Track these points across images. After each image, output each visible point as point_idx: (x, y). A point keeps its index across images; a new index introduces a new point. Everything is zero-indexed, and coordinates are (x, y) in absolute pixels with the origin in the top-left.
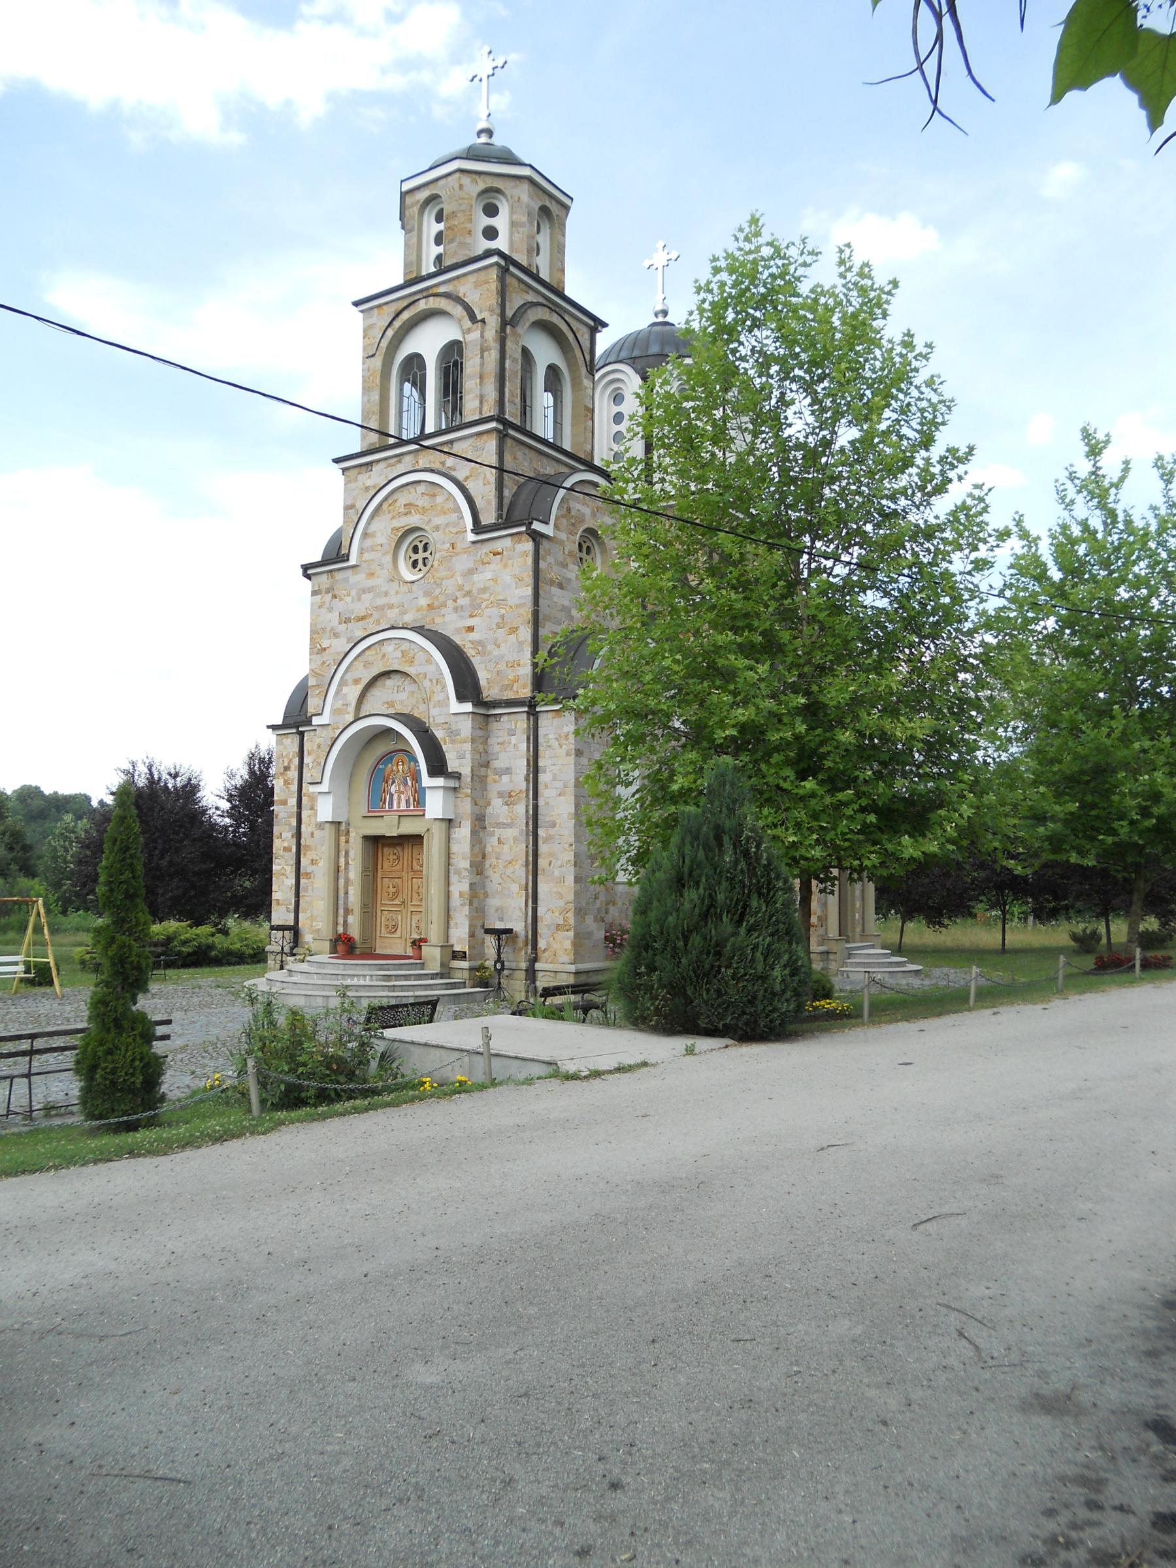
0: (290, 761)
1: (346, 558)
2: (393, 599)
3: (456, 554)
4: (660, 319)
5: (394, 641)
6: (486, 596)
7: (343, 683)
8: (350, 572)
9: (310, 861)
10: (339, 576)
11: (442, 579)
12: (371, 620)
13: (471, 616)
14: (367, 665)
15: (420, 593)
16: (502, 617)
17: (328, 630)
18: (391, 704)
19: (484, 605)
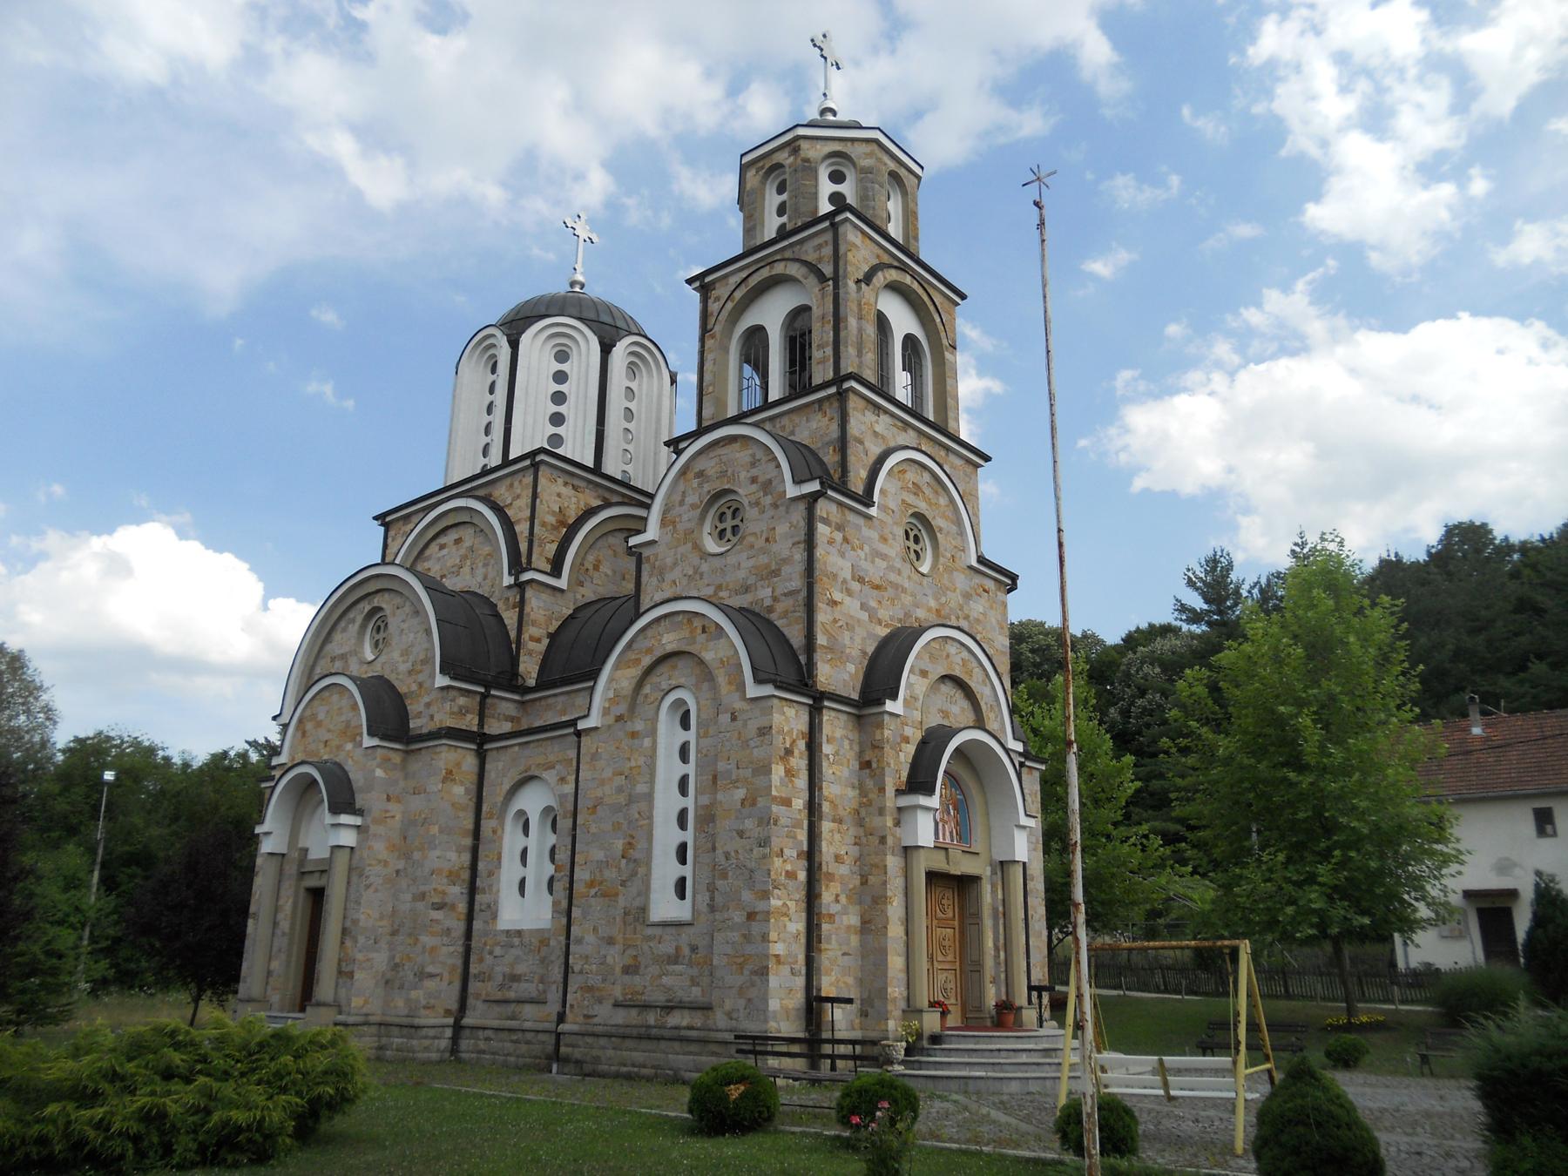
1: (867, 499)
2: (906, 585)
4: (577, 289)
5: (955, 644)
8: (861, 521)
10: (851, 517)
11: (947, 589)
15: (929, 592)
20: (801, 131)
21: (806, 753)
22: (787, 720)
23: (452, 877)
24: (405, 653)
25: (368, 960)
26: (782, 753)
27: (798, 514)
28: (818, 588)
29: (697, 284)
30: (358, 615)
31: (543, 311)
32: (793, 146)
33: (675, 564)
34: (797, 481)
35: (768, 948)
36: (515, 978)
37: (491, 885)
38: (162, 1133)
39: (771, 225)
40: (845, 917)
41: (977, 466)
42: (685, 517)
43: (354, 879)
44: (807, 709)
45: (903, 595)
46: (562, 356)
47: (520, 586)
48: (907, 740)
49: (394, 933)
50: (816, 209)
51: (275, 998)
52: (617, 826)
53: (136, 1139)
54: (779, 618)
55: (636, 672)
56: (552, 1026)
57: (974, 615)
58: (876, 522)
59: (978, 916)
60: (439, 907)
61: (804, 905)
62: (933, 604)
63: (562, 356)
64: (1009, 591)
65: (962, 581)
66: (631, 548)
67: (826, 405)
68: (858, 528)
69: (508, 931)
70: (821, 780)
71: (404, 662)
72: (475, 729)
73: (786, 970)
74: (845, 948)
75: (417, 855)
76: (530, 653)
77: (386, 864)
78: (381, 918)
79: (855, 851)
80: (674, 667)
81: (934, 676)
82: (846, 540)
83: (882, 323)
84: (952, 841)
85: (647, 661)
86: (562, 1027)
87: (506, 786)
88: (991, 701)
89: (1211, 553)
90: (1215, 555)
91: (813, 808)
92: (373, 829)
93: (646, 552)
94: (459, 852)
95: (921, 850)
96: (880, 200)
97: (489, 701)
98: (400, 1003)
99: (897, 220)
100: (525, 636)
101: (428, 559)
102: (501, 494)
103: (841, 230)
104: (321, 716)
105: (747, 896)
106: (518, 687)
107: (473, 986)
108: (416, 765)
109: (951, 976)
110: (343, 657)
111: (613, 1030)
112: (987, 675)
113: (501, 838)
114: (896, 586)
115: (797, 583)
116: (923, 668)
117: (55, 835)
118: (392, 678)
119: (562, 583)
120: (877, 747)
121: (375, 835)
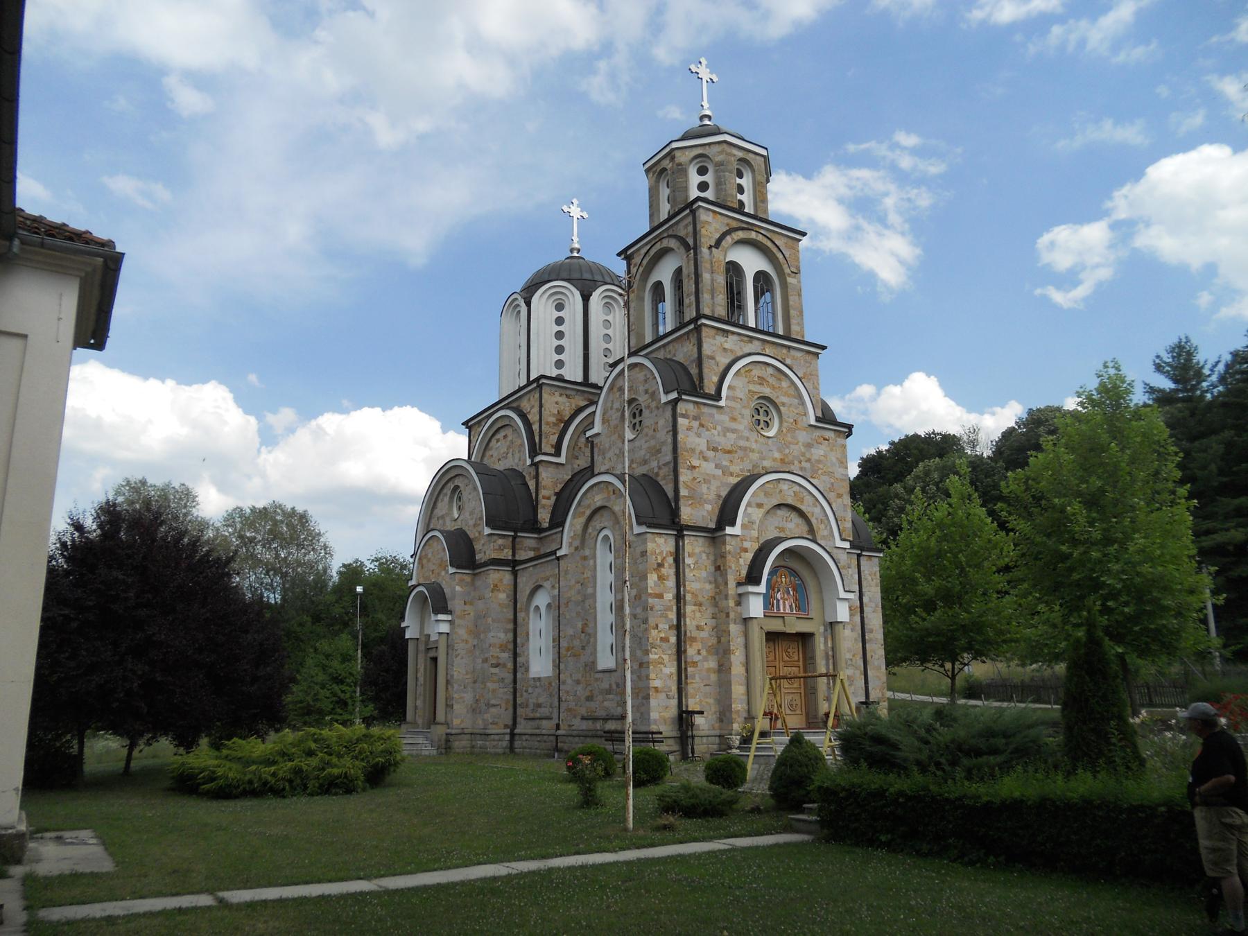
0: (664, 559)
1: (717, 396)
2: (754, 446)
3: (799, 429)
4: (575, 254)
5: (787, 482)
6: (821, 466)
7: (749, 505)
8: (714, 411)
9: (696, 651)
10: (705, 410)
11: (790, 443)
12: (736, 456)
13: (812, 477)
14: (767, 494)
16: (832, 484)
17: (697, 452)
18: (782, 529)
19: (820, 472)
20: (674, 145)
21: (674, 565)
22: (658, 546)
23: (503, 648)
24: (471, 513)
25: (461, 698)
26: (655, 567)
27: (668, 413)
28: (680, 460)
29: (623, 256)
30: (448, 491)
31: (546, 279)
32: (671, 155)
33: (610, 447)
34: (667, 392)
35: (649, 683)
36: (539, 706)
37: (523, 652)
38: (302, 779)
39: (665, 209)
40: (705, 663)
41: (817, 355)
42: (614, 418)
43: (450, 651)
44: (674, 538)
45: (751, 454)
46: (560, 307)
47: (535, 465)
48: (746, 550)
49: (475, 682)
50: (687, 197)
51: (420, 721)
52: (578, 614)
53: (291, 781)
54: (662, 480)
55: (582, 520)
56: (553, 732)
57: (815, 457)
58: (727, 410)
59: (813, 658)
60: (497, 666)
61: (675, 657)
62: (777, 455)
63: (560, 307)
64: (848, 436)
65: (803, 436)
66: (588, 438)
67: (691, 335)
68: (712, 416)
69: (534, 678)
70: (684, 581)
71: (472, 519)
72: (510, 558)
73: (663, 696)
74: (706, 682)
75: (482, 636)
76: (544, 507)
77: (467, 642)
78: (467, 674)
79: (712, 622)
80: (602, 516)
81: (767, 507)
82: (702, 425)
83: (734, 270)
84: (792, 611)
85: (588, 512)
86: (559, 732)
87: (528, 592)
88: (821, 516)
89: (1176, 341)
90: (1180, 342)
91: (679, 598)
92: (457, 622)
93: (596, 441)
94: (506, 632)
95: (754, 620)
96: (730, 183)
97: (518, 540)
98: (480, 722)
99: (749, 190)
100: (540, 497)
101: (491, 449)
102: (525, 405)
103: (697, 214)
104: (430, 555)
105: (639, 653)
106: (538, 528)
107: (519, 711)
108: (478, 583)
109: (797, 697)
110: (443, 517)
111: (581, 733)
112: (817, 500)
113: (528, 623)
114: (745, 449)
115: (669, 458)
116: (759, 502)
117: (337, 628)
118: (466, 529)
119: (562, 460)
120: (723, 556)
121: (459, 626)
